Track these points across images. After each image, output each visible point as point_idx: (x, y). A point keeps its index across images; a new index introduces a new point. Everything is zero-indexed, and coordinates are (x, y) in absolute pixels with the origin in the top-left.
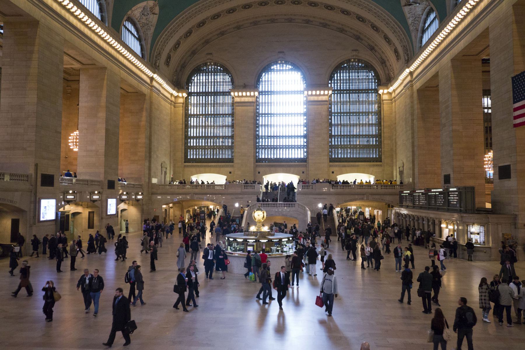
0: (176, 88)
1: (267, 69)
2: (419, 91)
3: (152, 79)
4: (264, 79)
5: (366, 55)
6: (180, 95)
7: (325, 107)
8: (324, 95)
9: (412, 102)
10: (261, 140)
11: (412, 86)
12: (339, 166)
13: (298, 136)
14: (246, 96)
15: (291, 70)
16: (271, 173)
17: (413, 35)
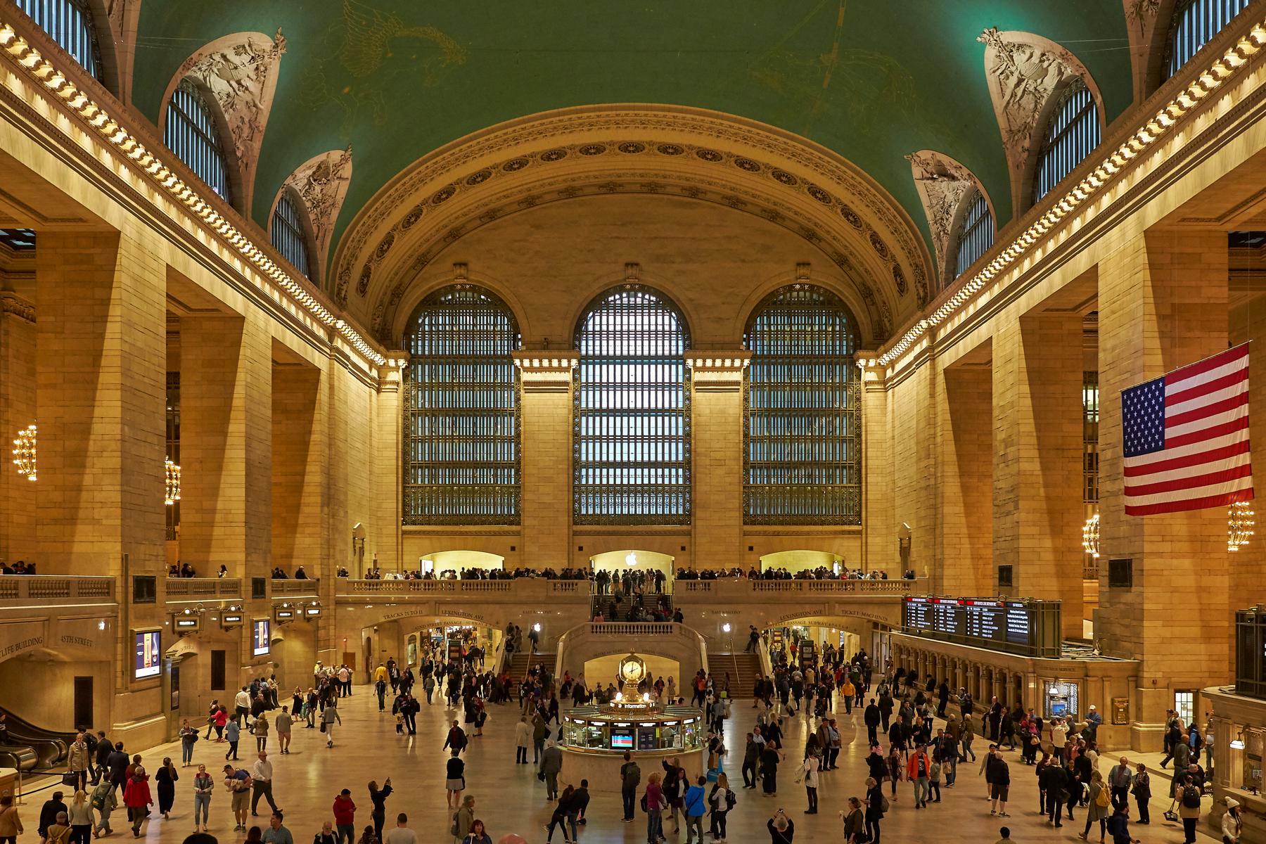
0: (382, 348)
1: (598, 303)
2: (946, 371)
3: (332, 332)
4: (590, 328)
5: (826, 277)
6: (392, 363)
7: (737, 397)
8: (732, 369)
9: (932, 395)
10: (584, 471)
11: (933, 359)
12: (765, 534)
13: (669, 465)
14: (550, 369)
15: (657, 306)
16: (609, 549)
17: (936, 245)
